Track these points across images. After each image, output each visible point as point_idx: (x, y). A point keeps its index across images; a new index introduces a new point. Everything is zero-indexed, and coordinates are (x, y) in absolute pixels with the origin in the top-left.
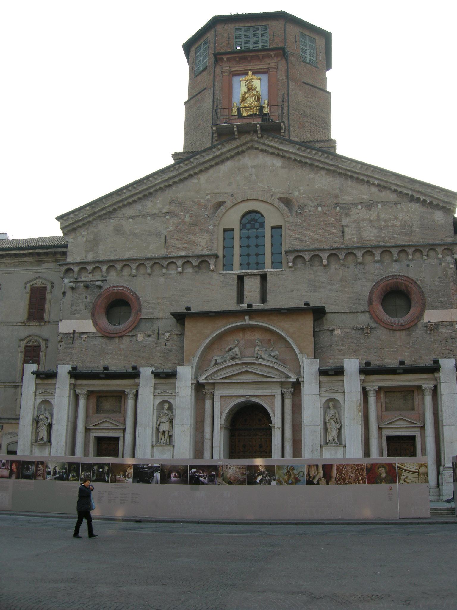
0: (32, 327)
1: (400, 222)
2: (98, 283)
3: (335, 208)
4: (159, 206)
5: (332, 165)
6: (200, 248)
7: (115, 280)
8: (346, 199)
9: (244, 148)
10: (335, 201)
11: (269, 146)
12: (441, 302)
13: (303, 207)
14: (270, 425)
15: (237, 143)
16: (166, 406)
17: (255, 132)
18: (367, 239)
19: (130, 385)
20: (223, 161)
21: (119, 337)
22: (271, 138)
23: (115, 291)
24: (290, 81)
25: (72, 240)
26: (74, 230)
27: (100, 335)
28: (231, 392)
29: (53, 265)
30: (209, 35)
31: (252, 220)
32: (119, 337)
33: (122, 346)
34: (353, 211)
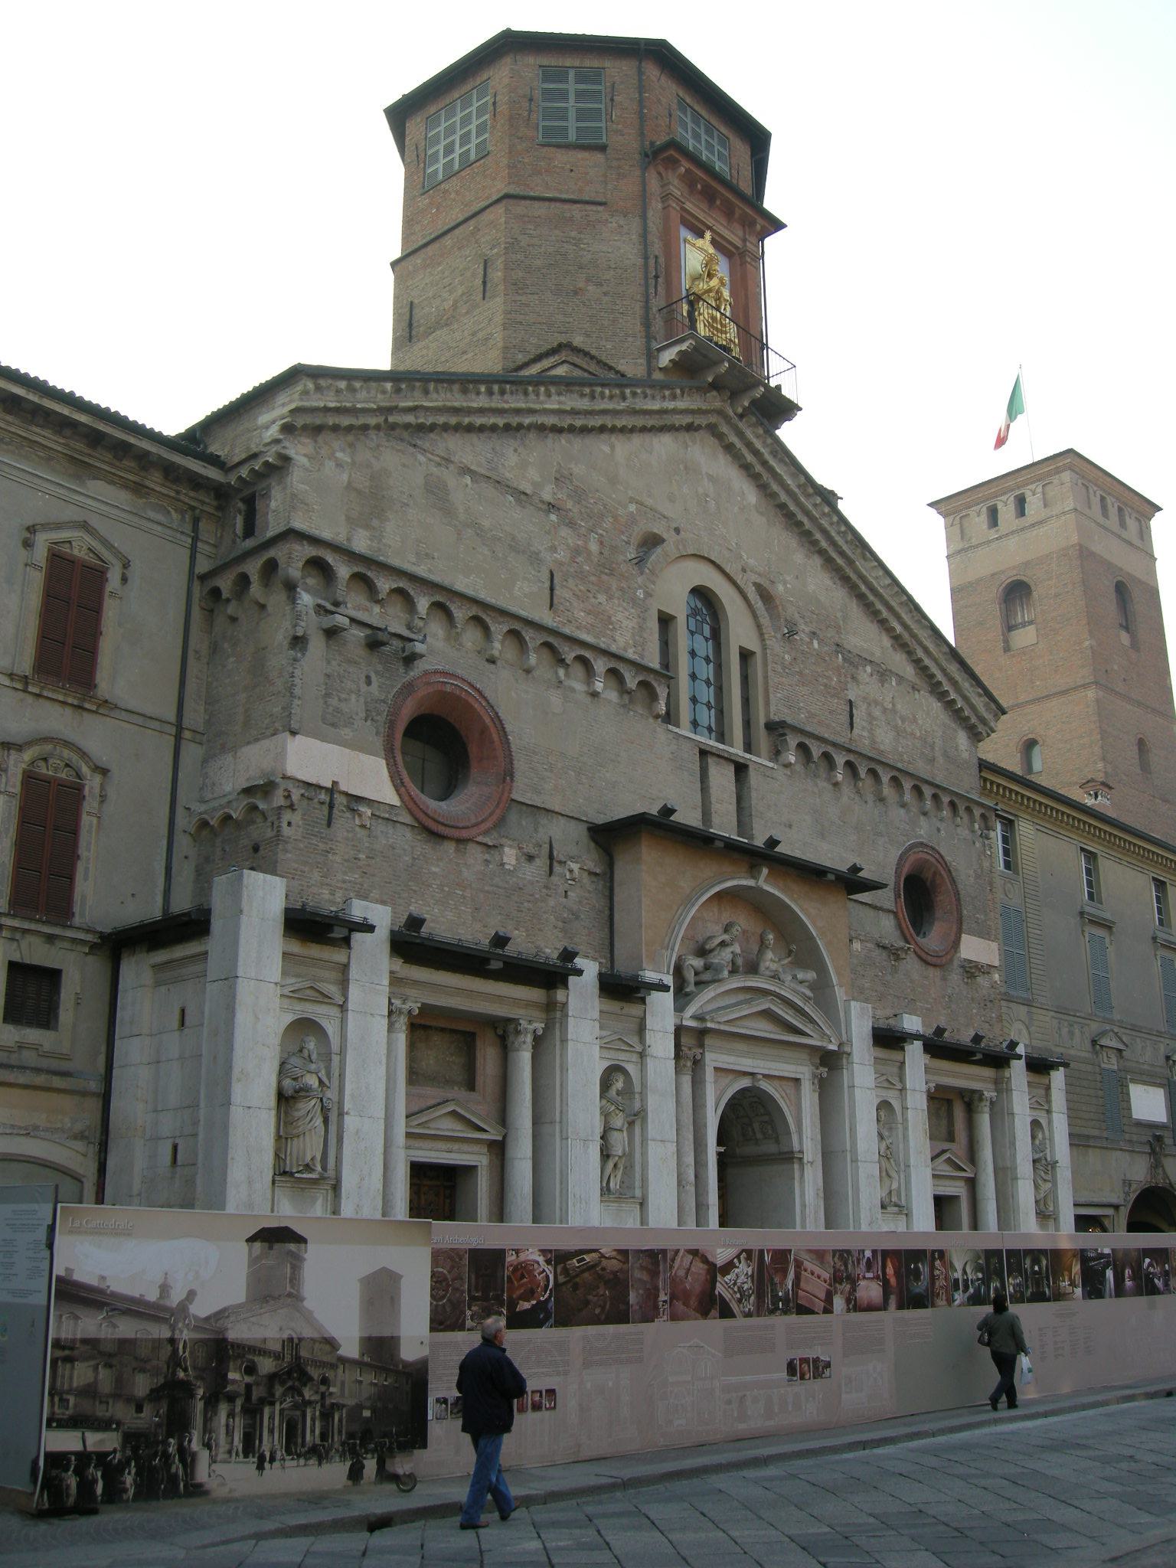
0: (47, 703)
5: (842, 553)
6: (621, 641)
7: (445, 652)
11: (749, 445)
19: (529, 1004)
21: (459, 841)
22: (761, 431)
23: (448, 689)
25: (304, 461)
26: (317, 430)
27: (406, 818)
28: (732, 1059)
29: (123, 497)
30: (607, 64)
33: (466, 873)
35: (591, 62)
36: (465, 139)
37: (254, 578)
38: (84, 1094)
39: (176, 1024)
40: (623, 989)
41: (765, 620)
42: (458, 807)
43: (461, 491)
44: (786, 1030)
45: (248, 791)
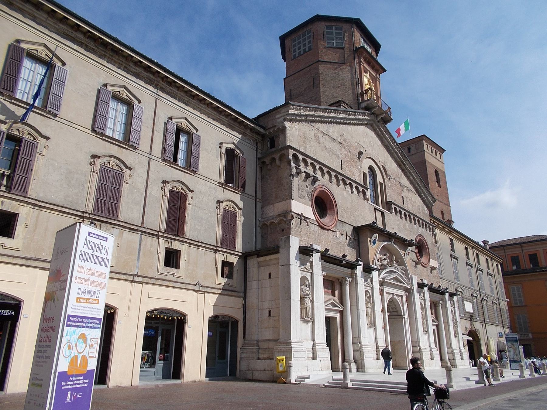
8: (402, 181)
11: (380, 129)
17: (377, 116)
35: (339, 24)
36: (304, 45)
37: (277, 159)
38: (240, 297)
39: (268, 277)
40: (368, 270)
41: (384, 175)
42: (326, 221)
43: (321, 138)
44: (397, 283)
45: (279, 215)
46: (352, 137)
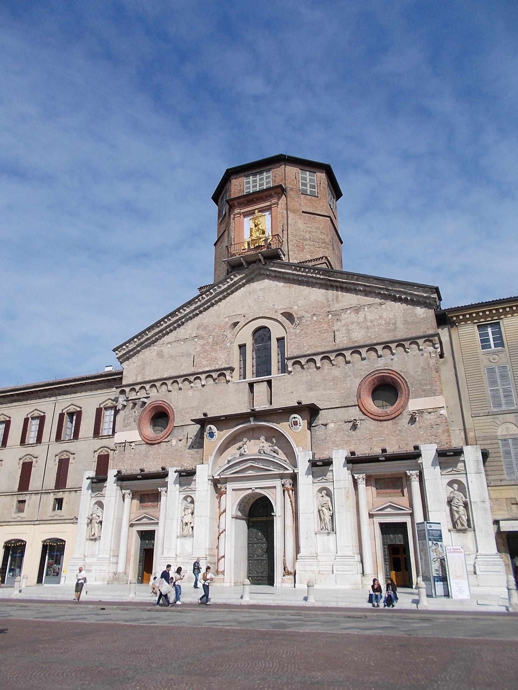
1: (385, 321)
2: (142, 400)
3: (328, 315)
4: (189, 331)
6: (220, 363)
7: (156, 396)
8: (337, 307)
9: (253, 276)
10: (328, 310)
12: (424, 390)
13: (300, 318)
14: (273, 514)
15: (247, 271)
16: (189, 500)
18: (356, 339)
20: (237, 289)
24: (289, 212)
26: (128, 359)
31: (262, 335)
32: (158, 443)
34: (343, 316)
46: (218, 317)
